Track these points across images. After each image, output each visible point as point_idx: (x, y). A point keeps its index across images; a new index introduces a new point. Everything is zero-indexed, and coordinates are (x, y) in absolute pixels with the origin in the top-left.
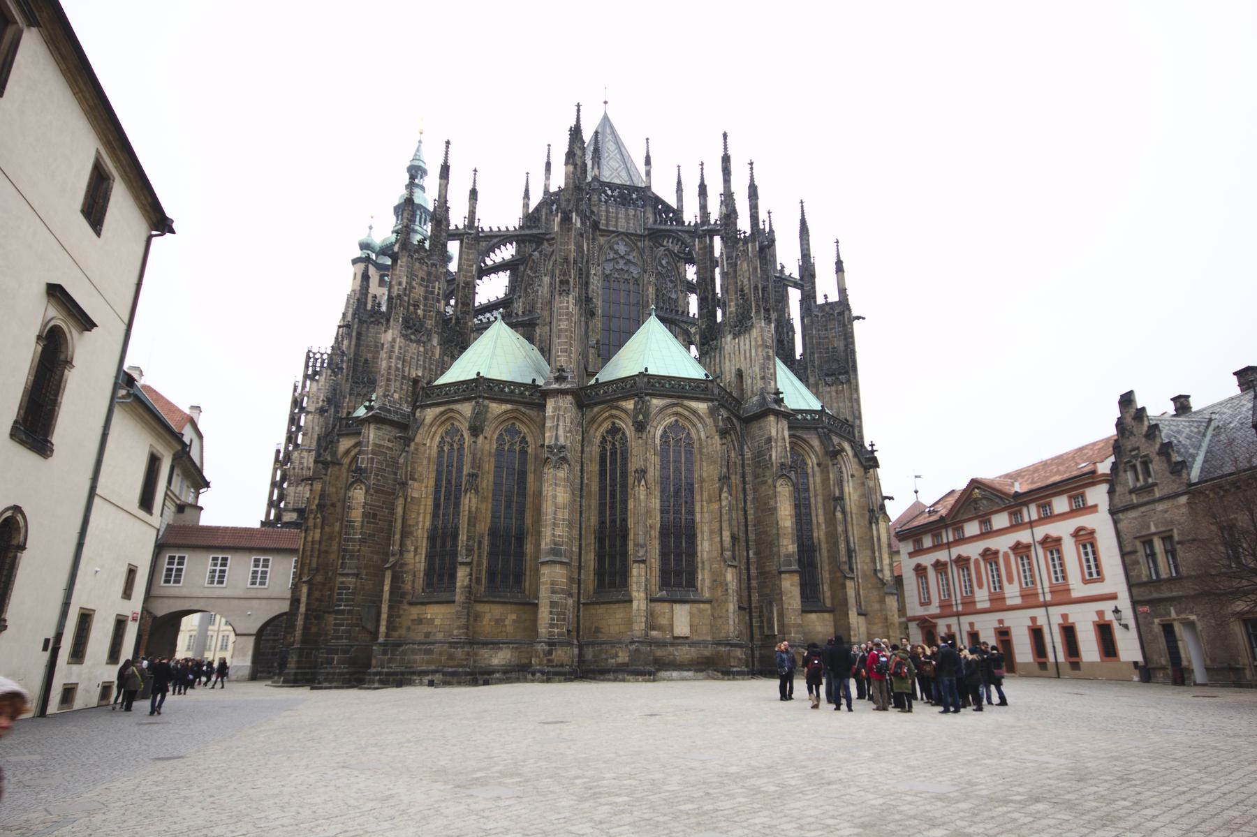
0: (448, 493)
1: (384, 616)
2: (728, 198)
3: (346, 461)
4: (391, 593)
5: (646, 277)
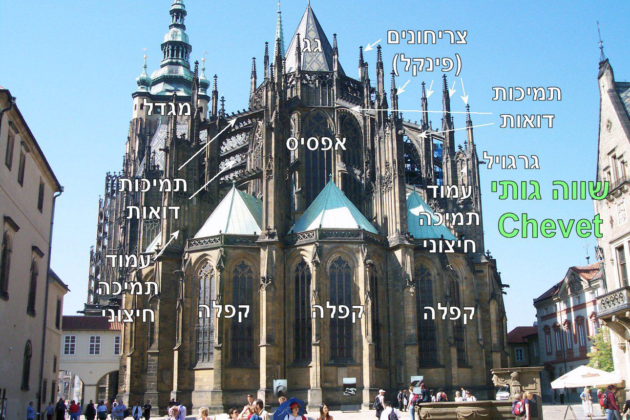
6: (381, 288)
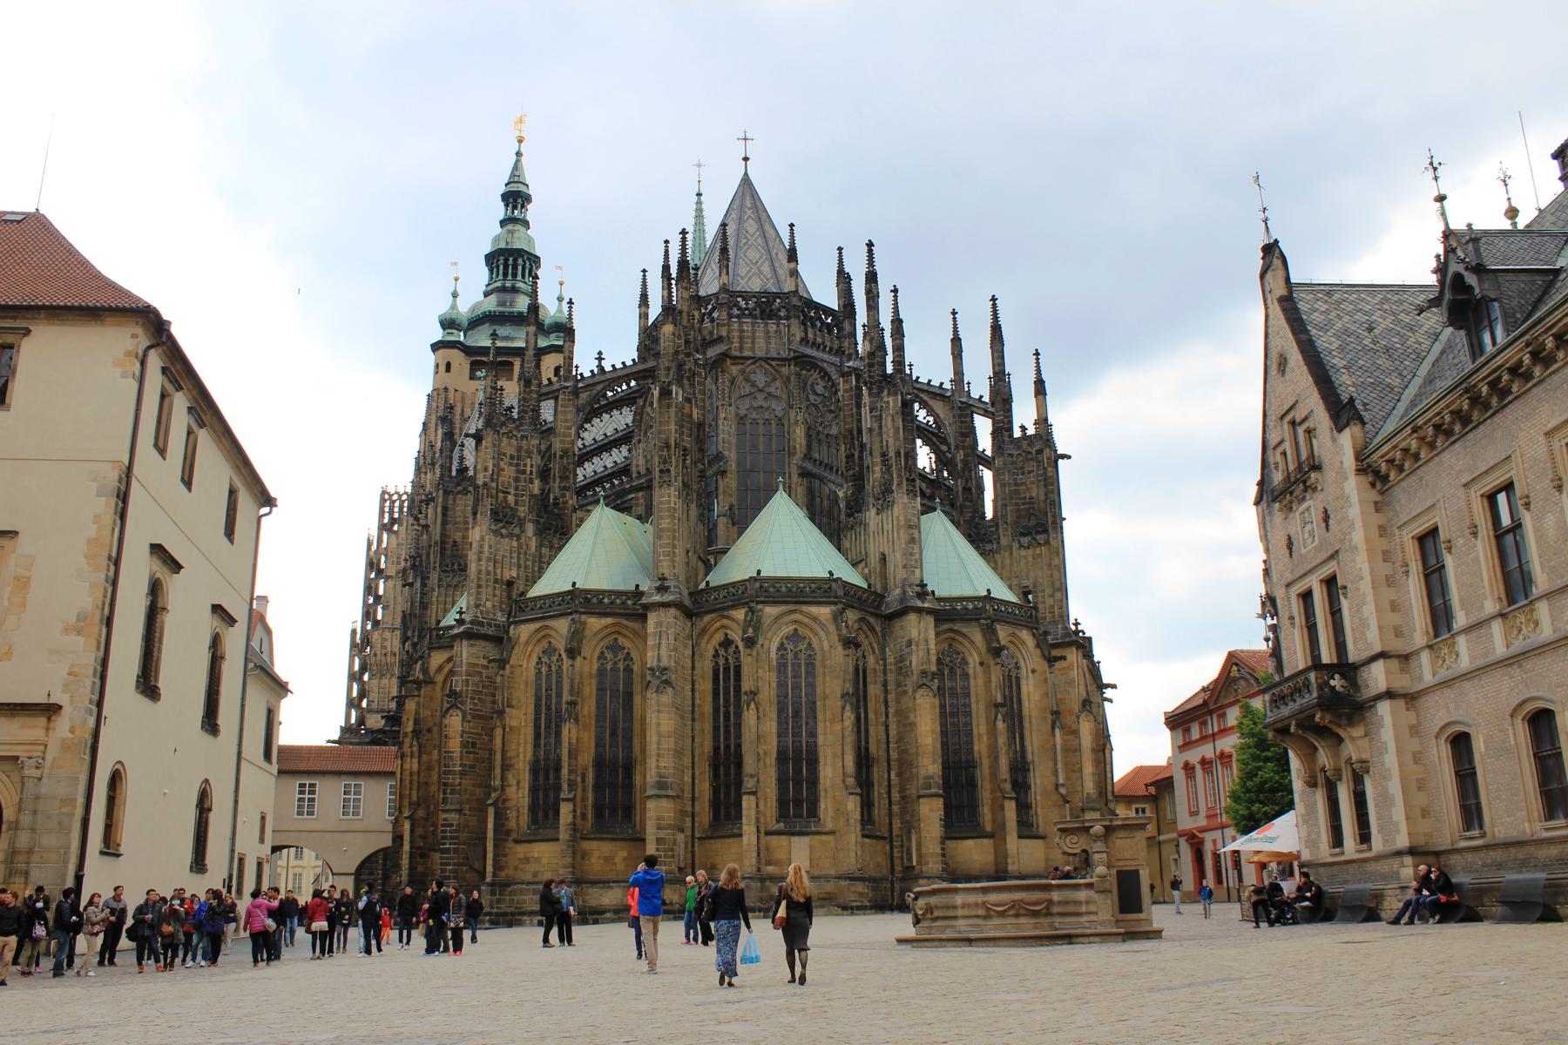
0: (549, 720)
1: (490, 856)
3: (440, 678)
4: (495, 831)
5: (792, 413)
6: (874, 689)
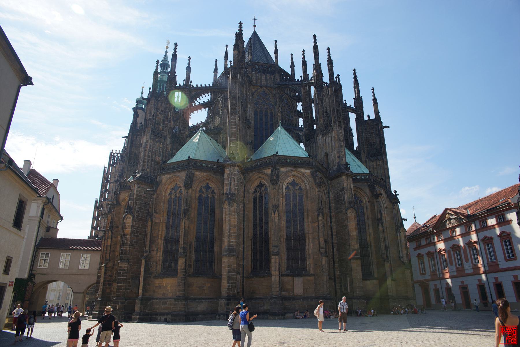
1: (141, 284)
2: (317, 66)
